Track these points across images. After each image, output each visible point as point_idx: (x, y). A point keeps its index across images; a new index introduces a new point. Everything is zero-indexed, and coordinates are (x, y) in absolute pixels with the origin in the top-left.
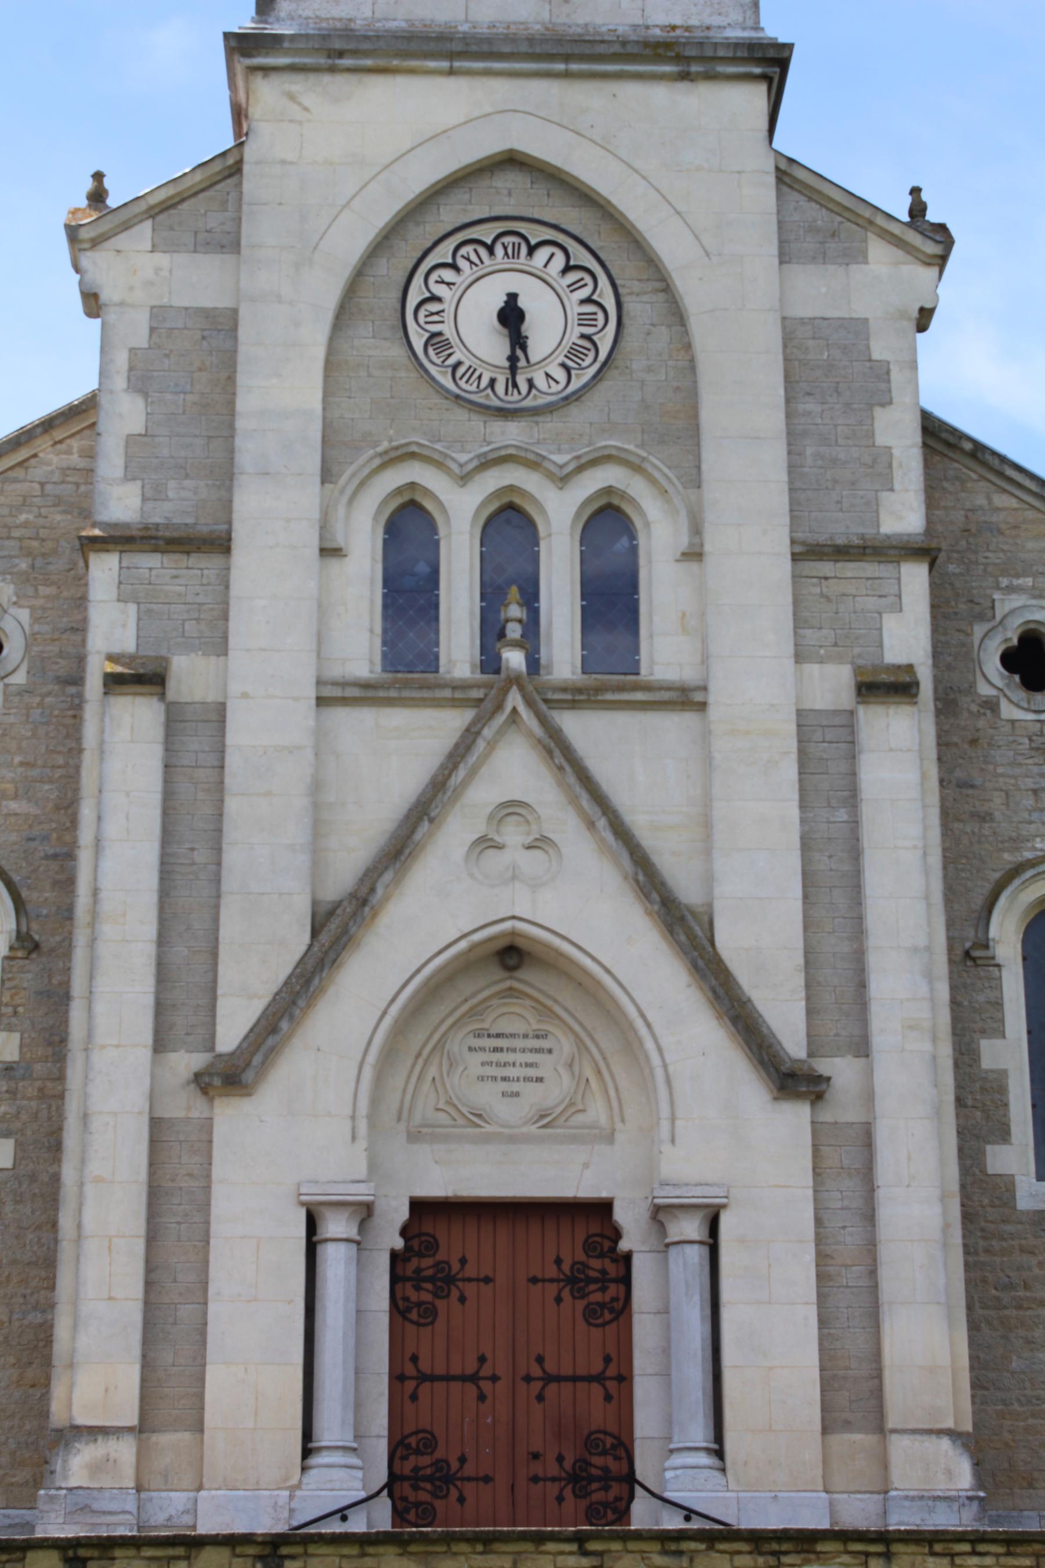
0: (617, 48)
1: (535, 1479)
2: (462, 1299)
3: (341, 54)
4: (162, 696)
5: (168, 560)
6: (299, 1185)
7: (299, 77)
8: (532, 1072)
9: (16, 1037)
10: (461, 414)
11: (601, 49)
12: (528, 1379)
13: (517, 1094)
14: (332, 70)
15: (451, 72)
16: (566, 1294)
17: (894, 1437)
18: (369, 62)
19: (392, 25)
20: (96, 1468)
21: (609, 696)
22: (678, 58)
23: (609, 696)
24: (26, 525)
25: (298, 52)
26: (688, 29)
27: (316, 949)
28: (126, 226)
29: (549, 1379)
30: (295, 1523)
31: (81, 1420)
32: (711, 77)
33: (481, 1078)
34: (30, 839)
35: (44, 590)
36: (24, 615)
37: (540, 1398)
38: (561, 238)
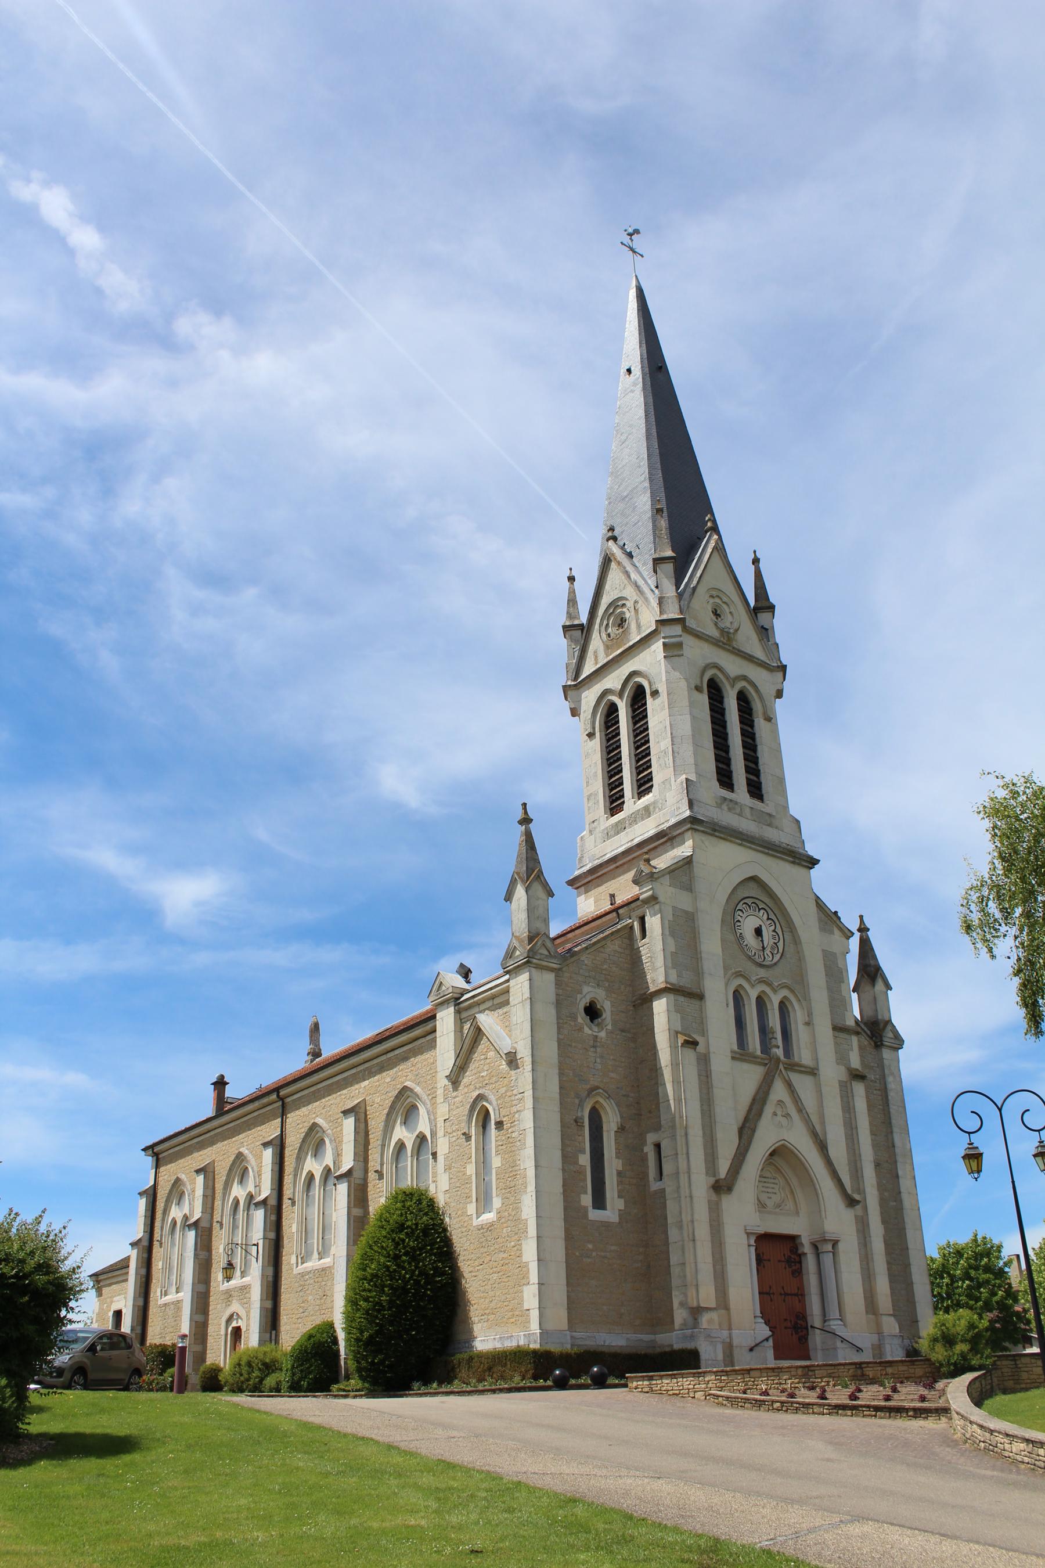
0: (781, 850)
1: (786, 1328)
2: (764, 1267)
3: (715, 830)
4: (695, 1049)
5: (687, 999)
6: (745, 1226)
7: (703, 835)
8: (774, 1191)
9: (621, 1161)
10: (750, 964)
11: (778, 849)
12: (781, 1294)
13: (771, 1198)
14: (712, 835)
15: (740, 845)
16: (787, 1266)
17: (883, 1316)
18: (722, 836)
19: (724, 823)
20: (710, 1321)
21: (796, 1068)
22: (794, 857)
23: (796, 1068)
24: (605, 970)
25: (706, 827)
26: (791, 846)
27: (742, 1145)
28: (663, 875)
29: (786, 1294)
30: (757, 1342)
31: (702, 1305)
32: (799, 864)
33: (763, 1192)
34: (618, 1088)
35: (614, 995)
36: (609, 1002)
37: (784, 1301)
38: (767, 908)
